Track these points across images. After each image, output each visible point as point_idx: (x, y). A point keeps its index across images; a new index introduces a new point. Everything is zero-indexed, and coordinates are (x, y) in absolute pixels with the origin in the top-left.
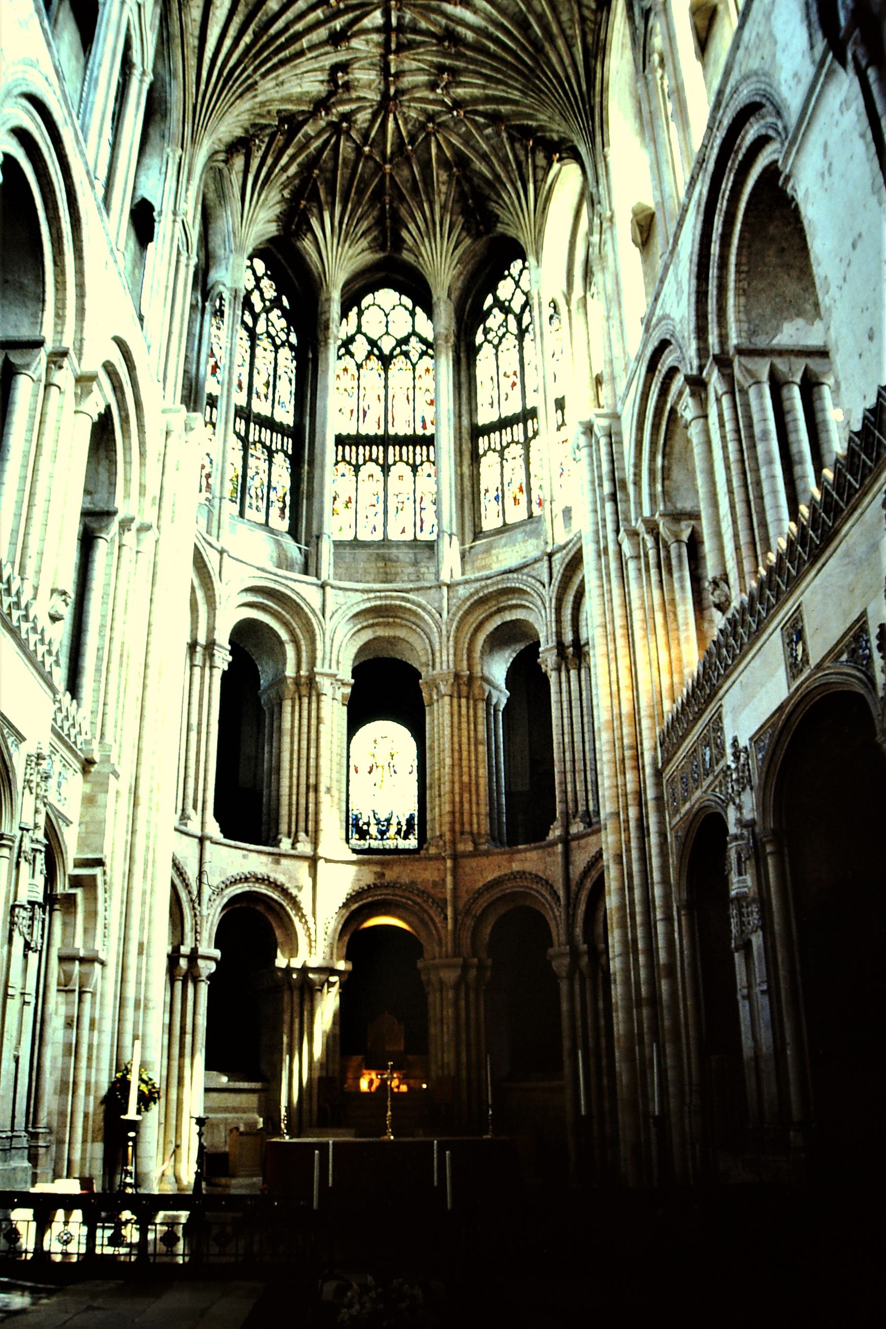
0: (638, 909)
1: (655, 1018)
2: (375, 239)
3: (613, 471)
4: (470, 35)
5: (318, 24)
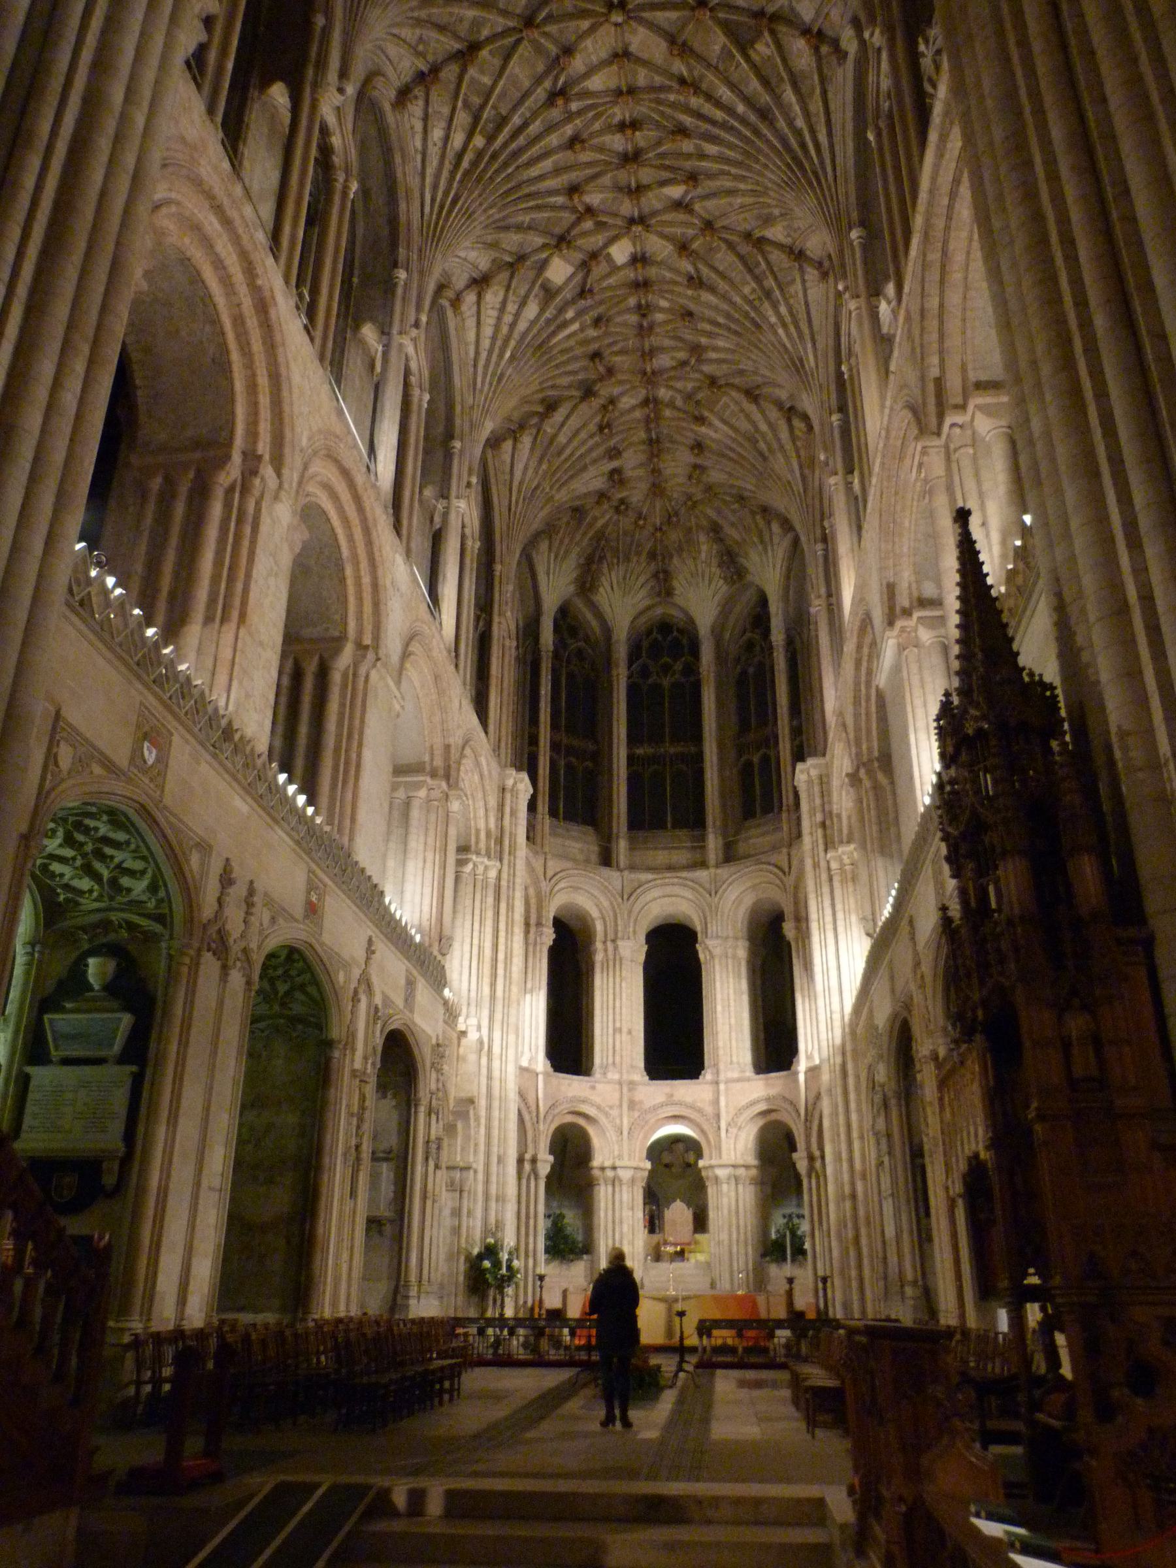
0: (842, 1130)
1: (855, 1209)
2: (652, 588)
3: (823, 805)
4: (714, 446)
5: (597, 445)
